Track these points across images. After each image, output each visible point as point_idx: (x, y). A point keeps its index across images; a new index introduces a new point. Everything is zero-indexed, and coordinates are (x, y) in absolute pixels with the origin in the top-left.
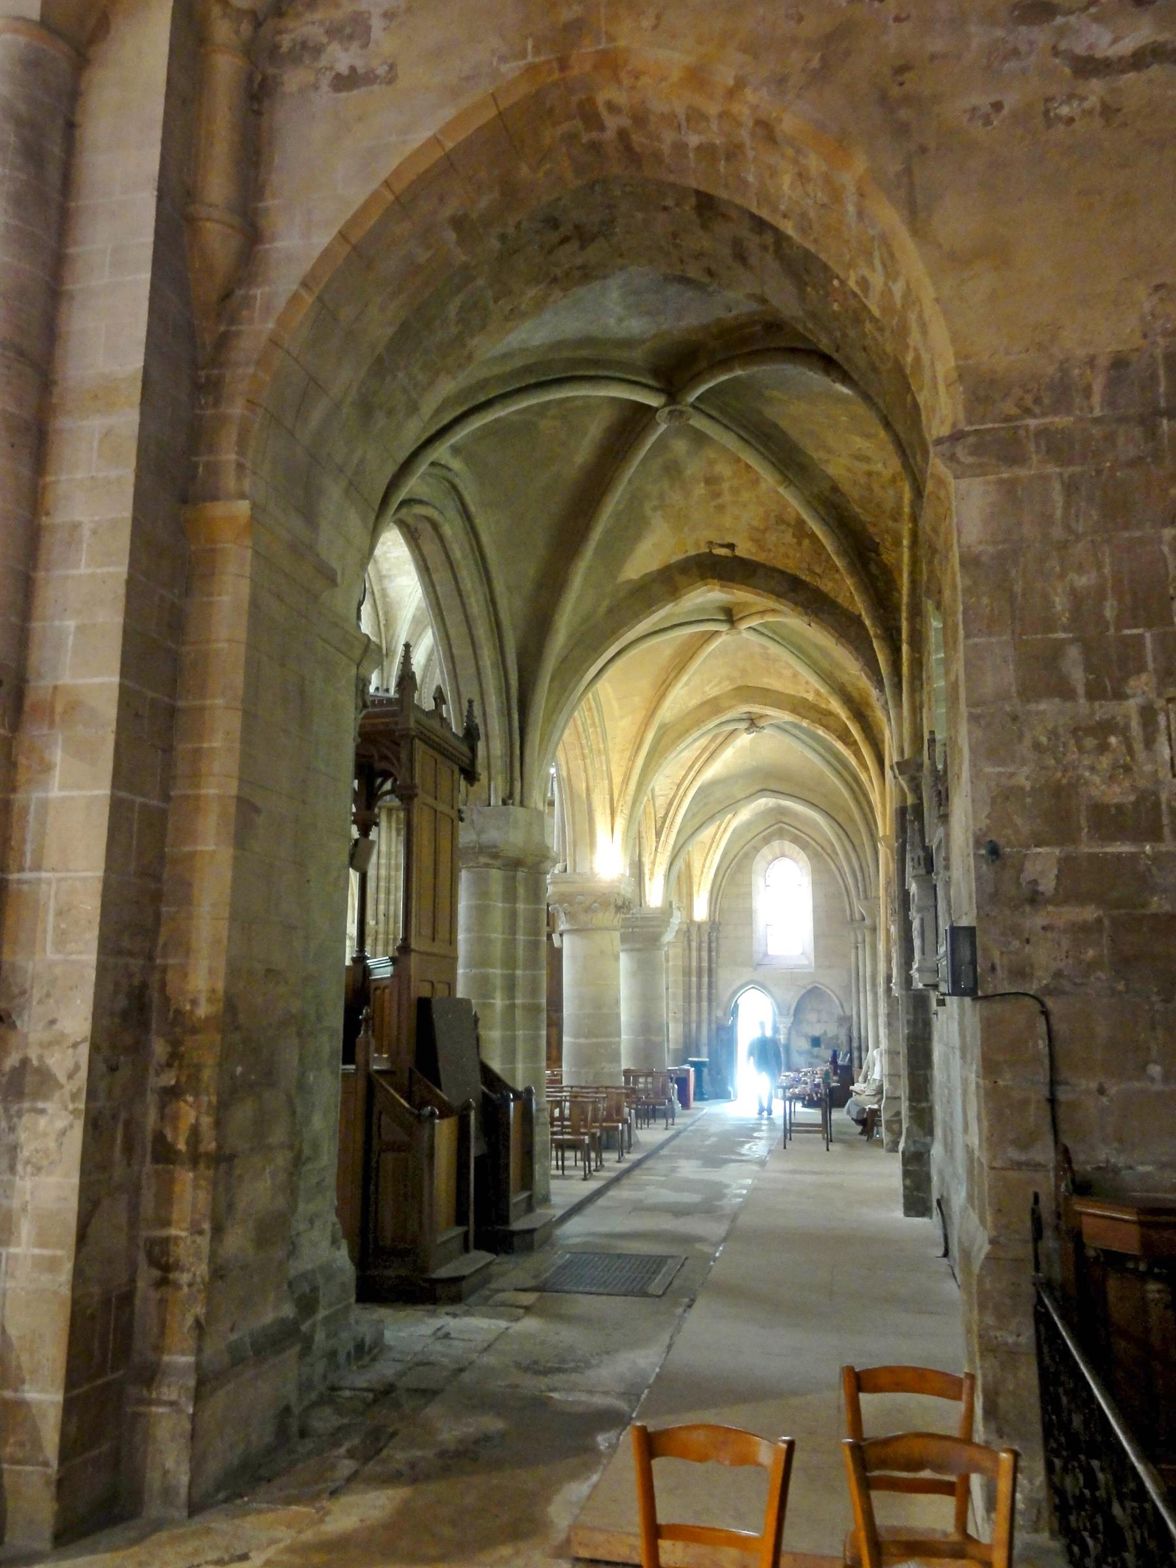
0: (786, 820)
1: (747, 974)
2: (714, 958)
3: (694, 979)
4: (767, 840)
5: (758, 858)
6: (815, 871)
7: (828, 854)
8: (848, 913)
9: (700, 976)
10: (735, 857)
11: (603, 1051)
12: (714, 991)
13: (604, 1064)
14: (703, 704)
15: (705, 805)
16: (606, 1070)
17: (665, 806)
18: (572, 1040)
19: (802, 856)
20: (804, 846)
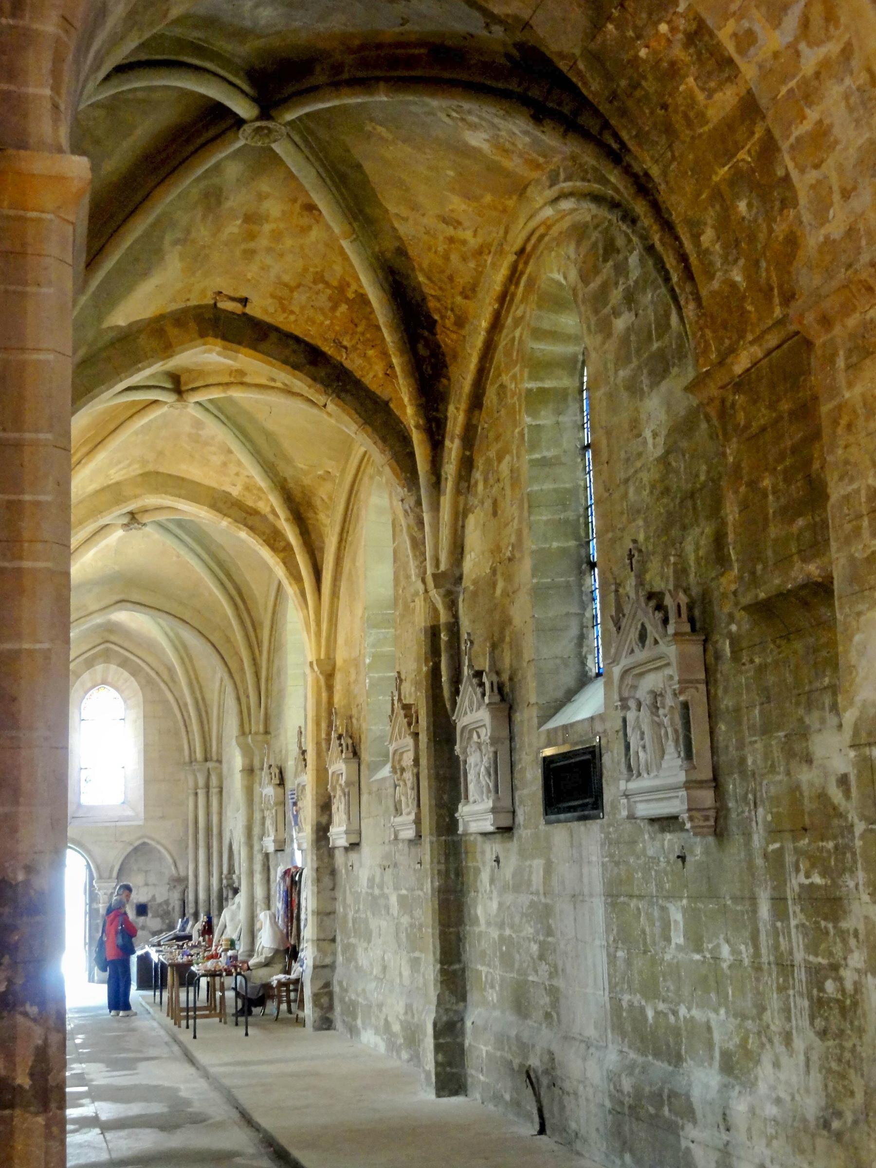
0: (113, 638)
7: (164, 681)
8: (186, 752)
14: (103, 490)
19: (133, 683)
20: (135, 672)
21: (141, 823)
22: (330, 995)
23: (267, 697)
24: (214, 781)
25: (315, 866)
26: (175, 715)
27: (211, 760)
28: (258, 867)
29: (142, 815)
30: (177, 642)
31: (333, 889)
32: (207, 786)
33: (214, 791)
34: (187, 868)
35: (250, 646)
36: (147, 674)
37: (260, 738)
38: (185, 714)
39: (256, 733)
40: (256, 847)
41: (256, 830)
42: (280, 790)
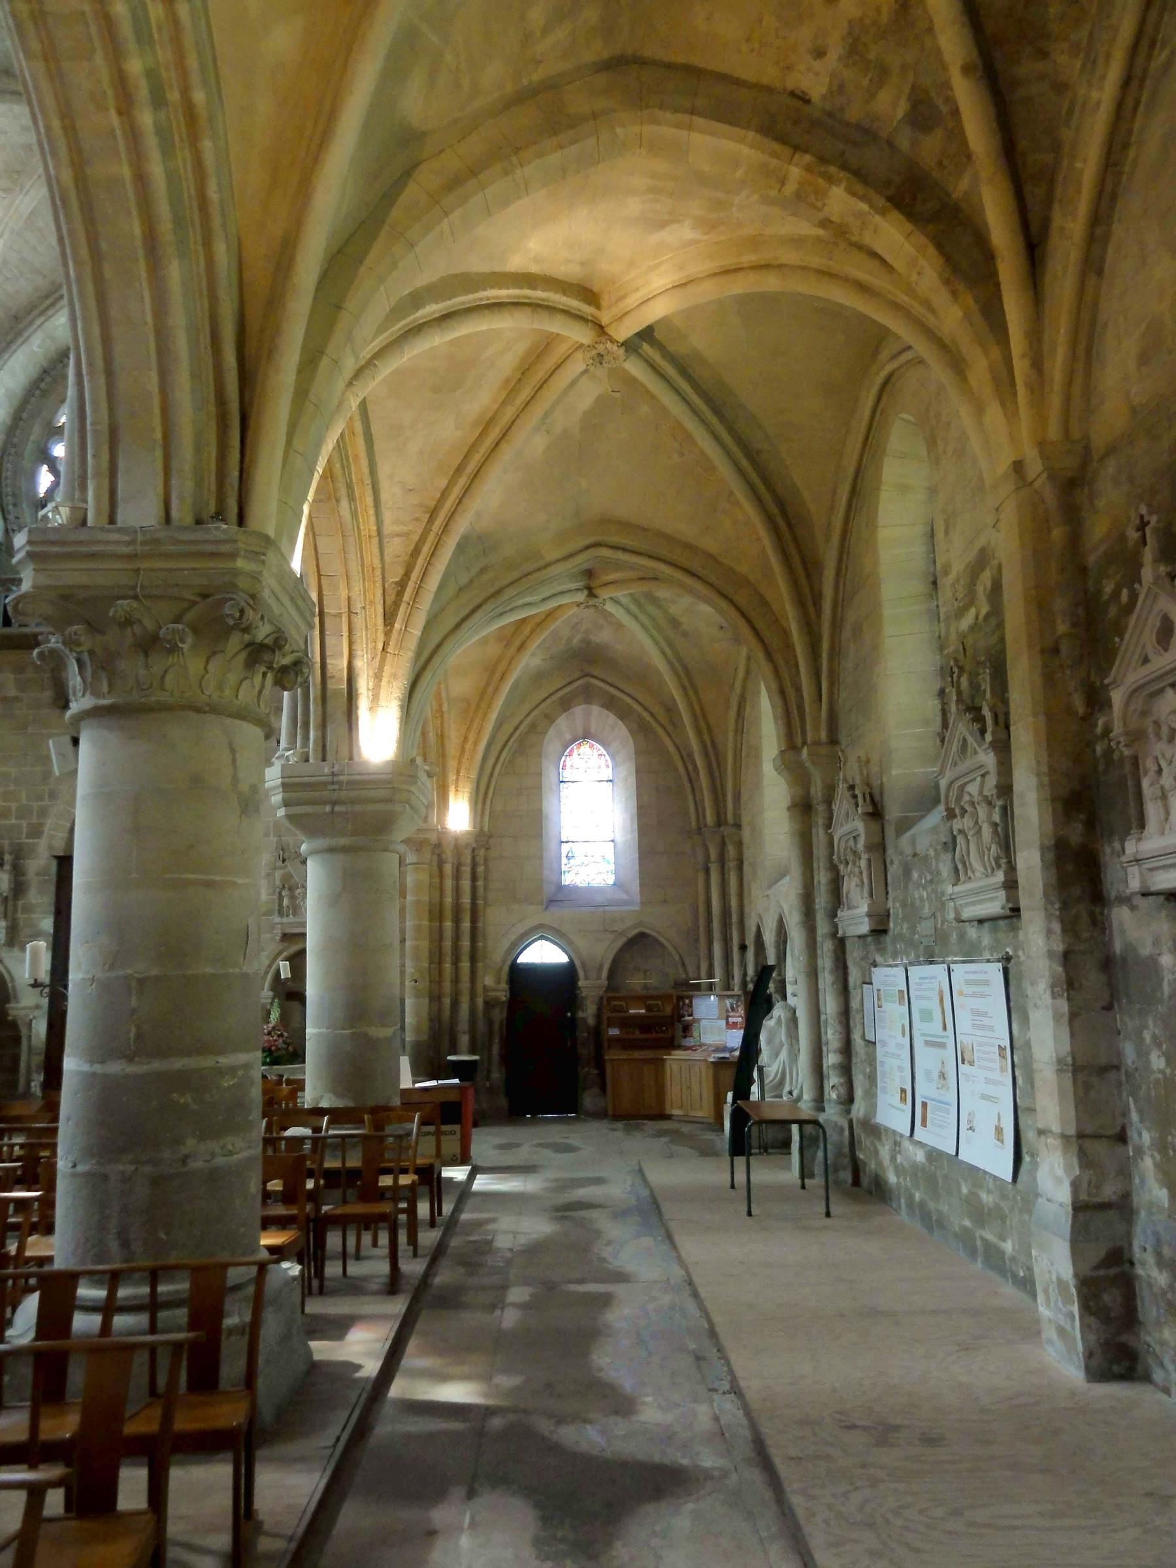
1: (534, 915)
2: (481, 891)
3: (448, 924)
4: (566, 704)
5: (551, 732)
6: (641, 754)
7: (661, 725)
9: (457, 921)
10: (516, 728)
11: (186, 1099)
13: (191, 1142)
15: (483, 570)
16: (197, 1164)
18: (86, 1068)
19: (622, 730)
20: (623, 714)
22: (1127, 1284)
23: (832, 684)
24: (731, 850)
25: (1059, 948)
26: (676, 770)
27: (726, 823)
28: (826, 962)
30: (677, 665)
31: (1109, 1008)
32: (722, 860)
33: (731, 865)
35: (801, 603)
36: (639, 716)
37: (823, 751)
38: (690, 767)
39: (817, 743)
40: (822, 928)
41: (822, 901)
42: (875, 826)
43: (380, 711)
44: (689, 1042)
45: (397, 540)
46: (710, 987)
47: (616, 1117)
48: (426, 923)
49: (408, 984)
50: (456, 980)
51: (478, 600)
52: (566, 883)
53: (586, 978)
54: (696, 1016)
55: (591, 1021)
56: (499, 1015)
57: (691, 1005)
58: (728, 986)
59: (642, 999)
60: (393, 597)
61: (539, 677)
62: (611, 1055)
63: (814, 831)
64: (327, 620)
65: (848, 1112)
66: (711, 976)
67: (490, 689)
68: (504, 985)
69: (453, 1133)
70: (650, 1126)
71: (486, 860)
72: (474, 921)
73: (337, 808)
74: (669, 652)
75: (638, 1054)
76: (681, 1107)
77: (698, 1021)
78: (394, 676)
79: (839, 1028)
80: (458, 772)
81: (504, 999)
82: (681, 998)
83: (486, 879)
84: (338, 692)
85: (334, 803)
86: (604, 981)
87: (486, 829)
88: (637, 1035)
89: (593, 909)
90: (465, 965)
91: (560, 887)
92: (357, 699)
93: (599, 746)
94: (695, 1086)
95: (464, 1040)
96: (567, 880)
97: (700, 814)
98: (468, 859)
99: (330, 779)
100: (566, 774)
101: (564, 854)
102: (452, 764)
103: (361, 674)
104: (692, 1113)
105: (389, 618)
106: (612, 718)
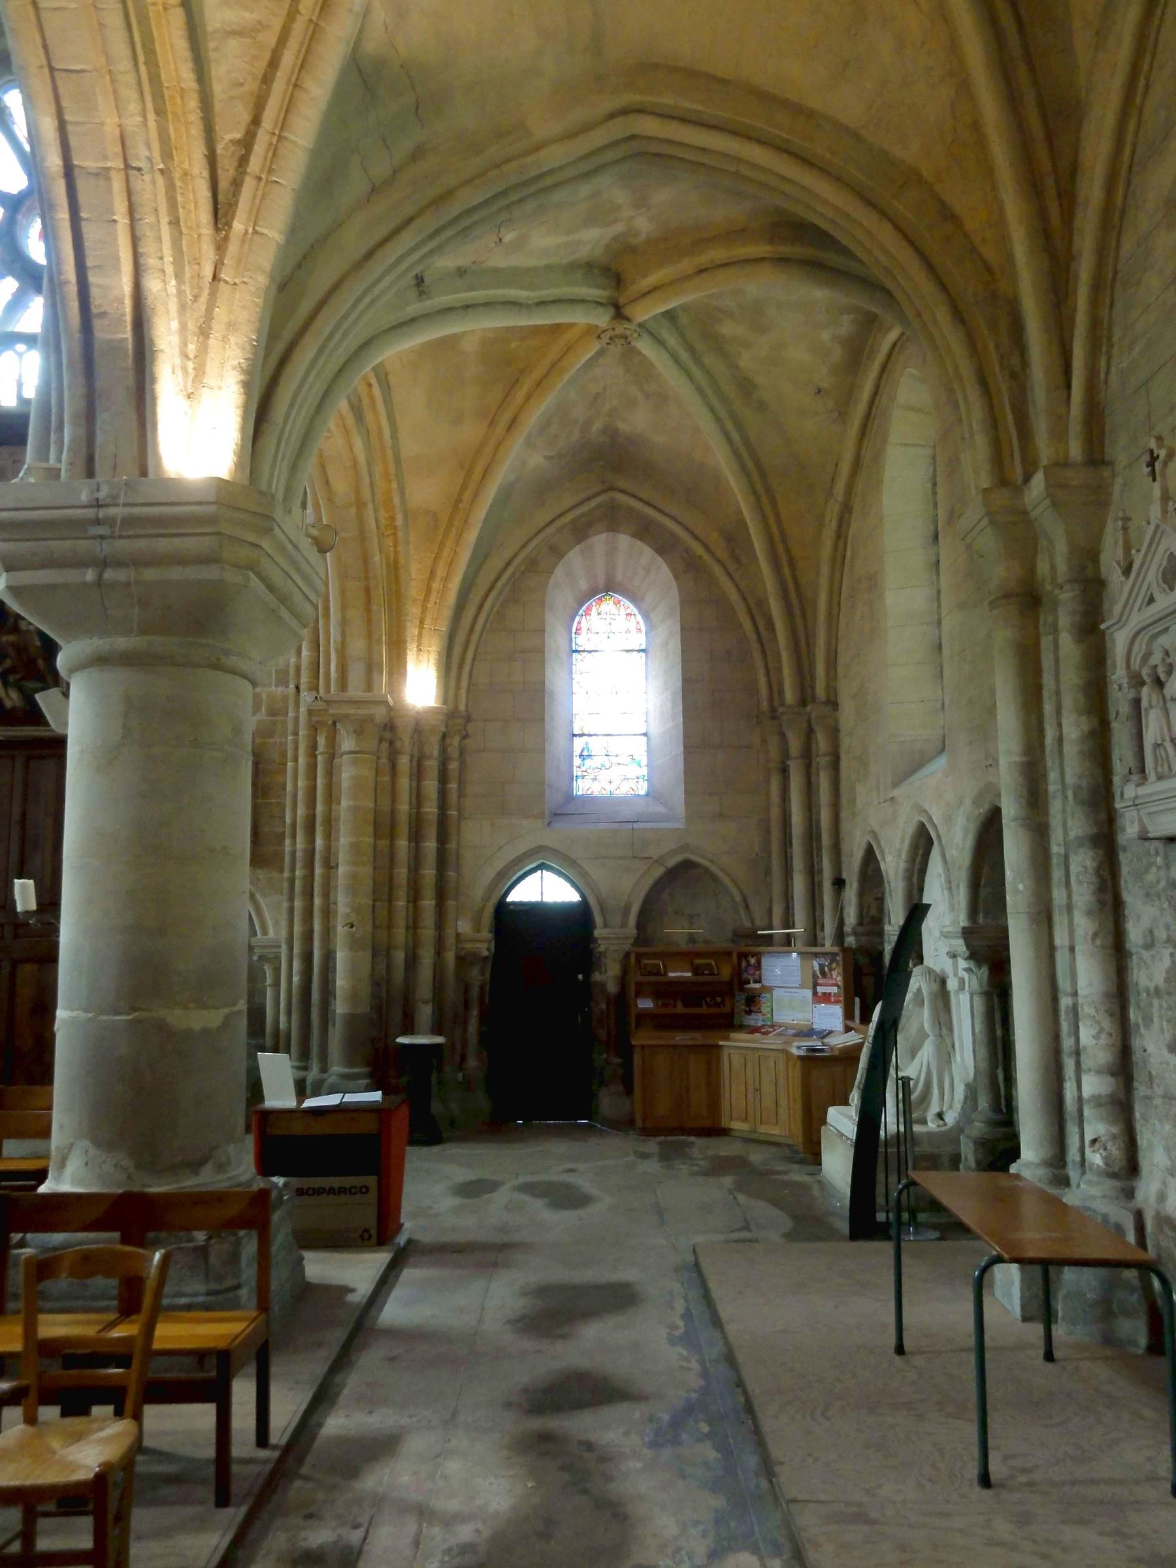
1: (531, 834)
2: (453, 797)
3: (403, 844)
4: (581, 532)
5: (559, 573)
8: (764, 692)
9: (416, 836)
10: (508, 564)
12: (451, 874)
15: (417, 155)
17: (252, 85)
19: (663, 572)
20: (665, 546)
21: (680, 825)
24: (822, 742)
27: (814, 699)
29: (681, 810)
32: (807, 755)
33: (823, 761)
34: (770, 911)
36: (687, 550)
38: (761, 624)
43: (205, 395)
44: (755, 1020)
45: (233, 44)
46: (788, 940)
47: (648, 1132)
48: (368, 840)
49: (341, 931)
50: (414, 925)
51: (410, 210)
52: (580, 793)
53: (606, 925)
54: (765, 983)
55: (612, 988)
56: (478, 976)
57: (758, 966)
58: (813, 939)
59: (687, 957)
60: (231, 172)
61: (542, 488)
62: (641, 1039)
63: (1046, 642)
64: (81, 184)
65: (1129, 1194)
66: (788, 923)
67: (467, 495)
68: (486, 934)
69: (364, 1190)
70: (699, 1146)
71: (462, 752)
72: (442, 839)
73: (109, 575)
74: (735, 436)
75: (681, 1038)
76: (745, 1119)
77: (770, 990)
78: (231, 326)
79: (1107, 1024)
80: (421, 628)
81: (486, 953)
82: (743, 956)
83: (461, 782)
84: (115, 347)
85: (103, 564)
86: (631, 929)
87: (462, 708)
88: (680, 1009)
89: (616, 826)
90: (428, 903)
91: (570, 798)
92: (153, 361)
93: (628, 603)
94: (768, 1088)
95: (425, 1013)
96: (581, 787)
97: (774, 690)
98: (434, 749)
99: (90, 513)
100: (581, 641)
101: (577, 750)
102: (413, 610)
103: (160, 309)
104: (763, 1129)
105: (221, 214)
106: (647, 553)
